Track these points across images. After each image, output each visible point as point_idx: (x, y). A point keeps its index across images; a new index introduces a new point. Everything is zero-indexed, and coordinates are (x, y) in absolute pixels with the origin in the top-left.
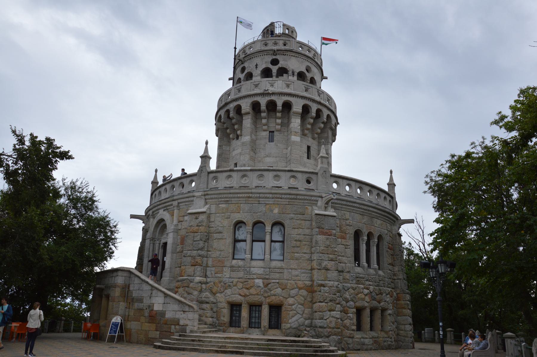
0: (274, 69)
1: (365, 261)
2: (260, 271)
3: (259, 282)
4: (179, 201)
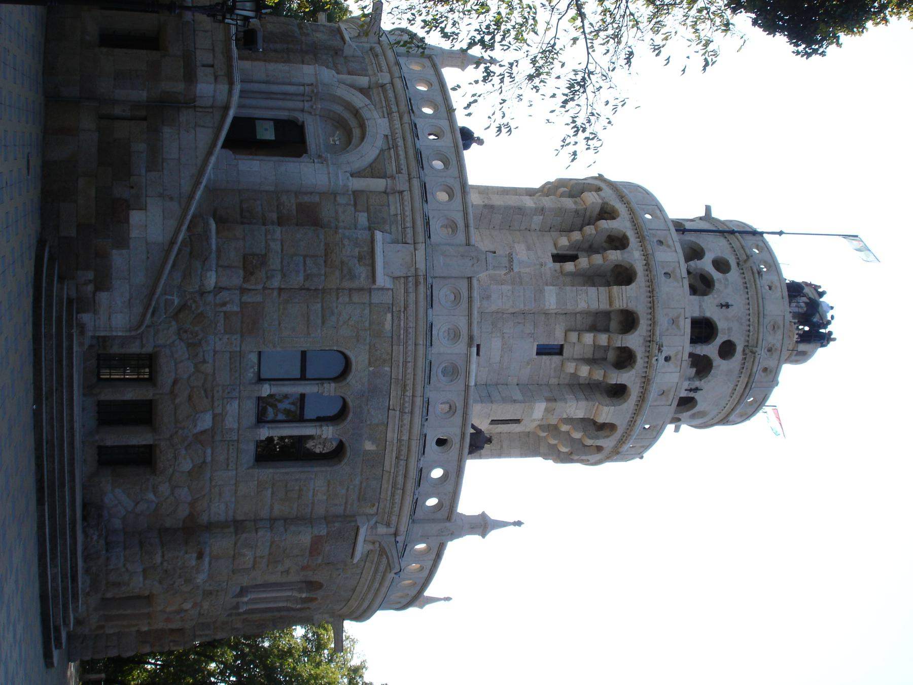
0: (710, 350)
1: (252, 597)
2: (230, 422)
3: (205, 422)
4: (407, 195)
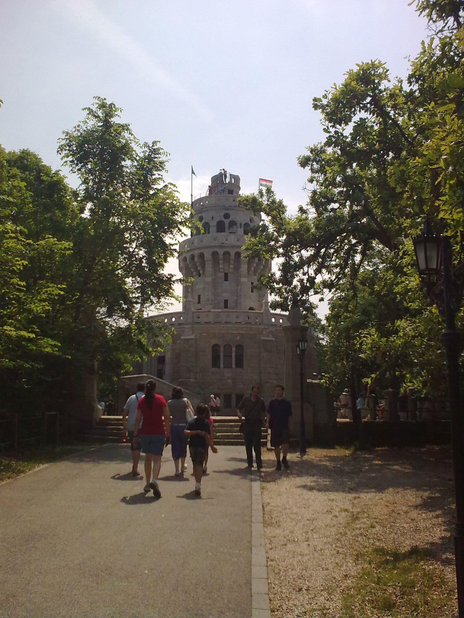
0: (227, 222)
3: (230, 381)
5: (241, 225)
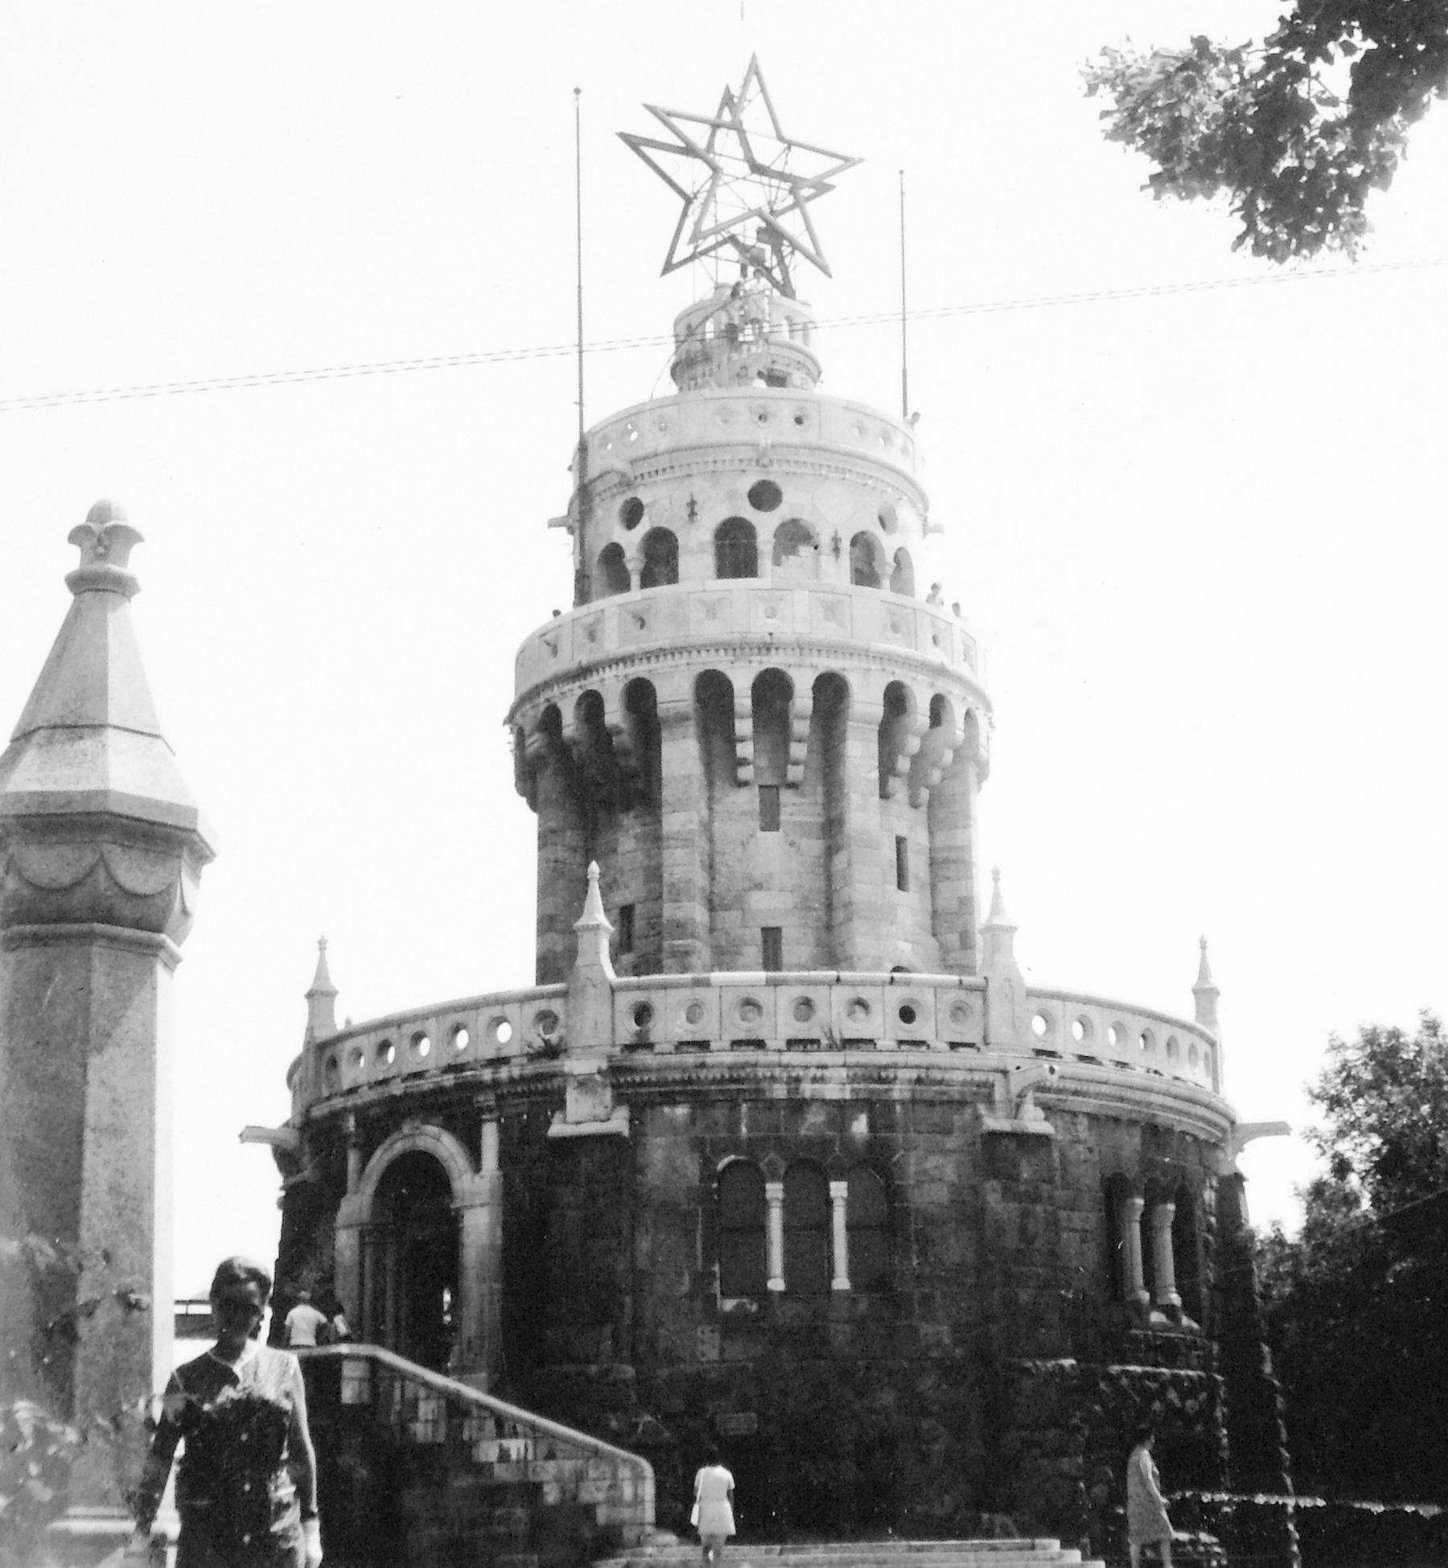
0: (765, 525)
5: (836, 540)
